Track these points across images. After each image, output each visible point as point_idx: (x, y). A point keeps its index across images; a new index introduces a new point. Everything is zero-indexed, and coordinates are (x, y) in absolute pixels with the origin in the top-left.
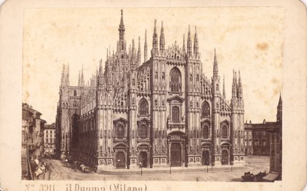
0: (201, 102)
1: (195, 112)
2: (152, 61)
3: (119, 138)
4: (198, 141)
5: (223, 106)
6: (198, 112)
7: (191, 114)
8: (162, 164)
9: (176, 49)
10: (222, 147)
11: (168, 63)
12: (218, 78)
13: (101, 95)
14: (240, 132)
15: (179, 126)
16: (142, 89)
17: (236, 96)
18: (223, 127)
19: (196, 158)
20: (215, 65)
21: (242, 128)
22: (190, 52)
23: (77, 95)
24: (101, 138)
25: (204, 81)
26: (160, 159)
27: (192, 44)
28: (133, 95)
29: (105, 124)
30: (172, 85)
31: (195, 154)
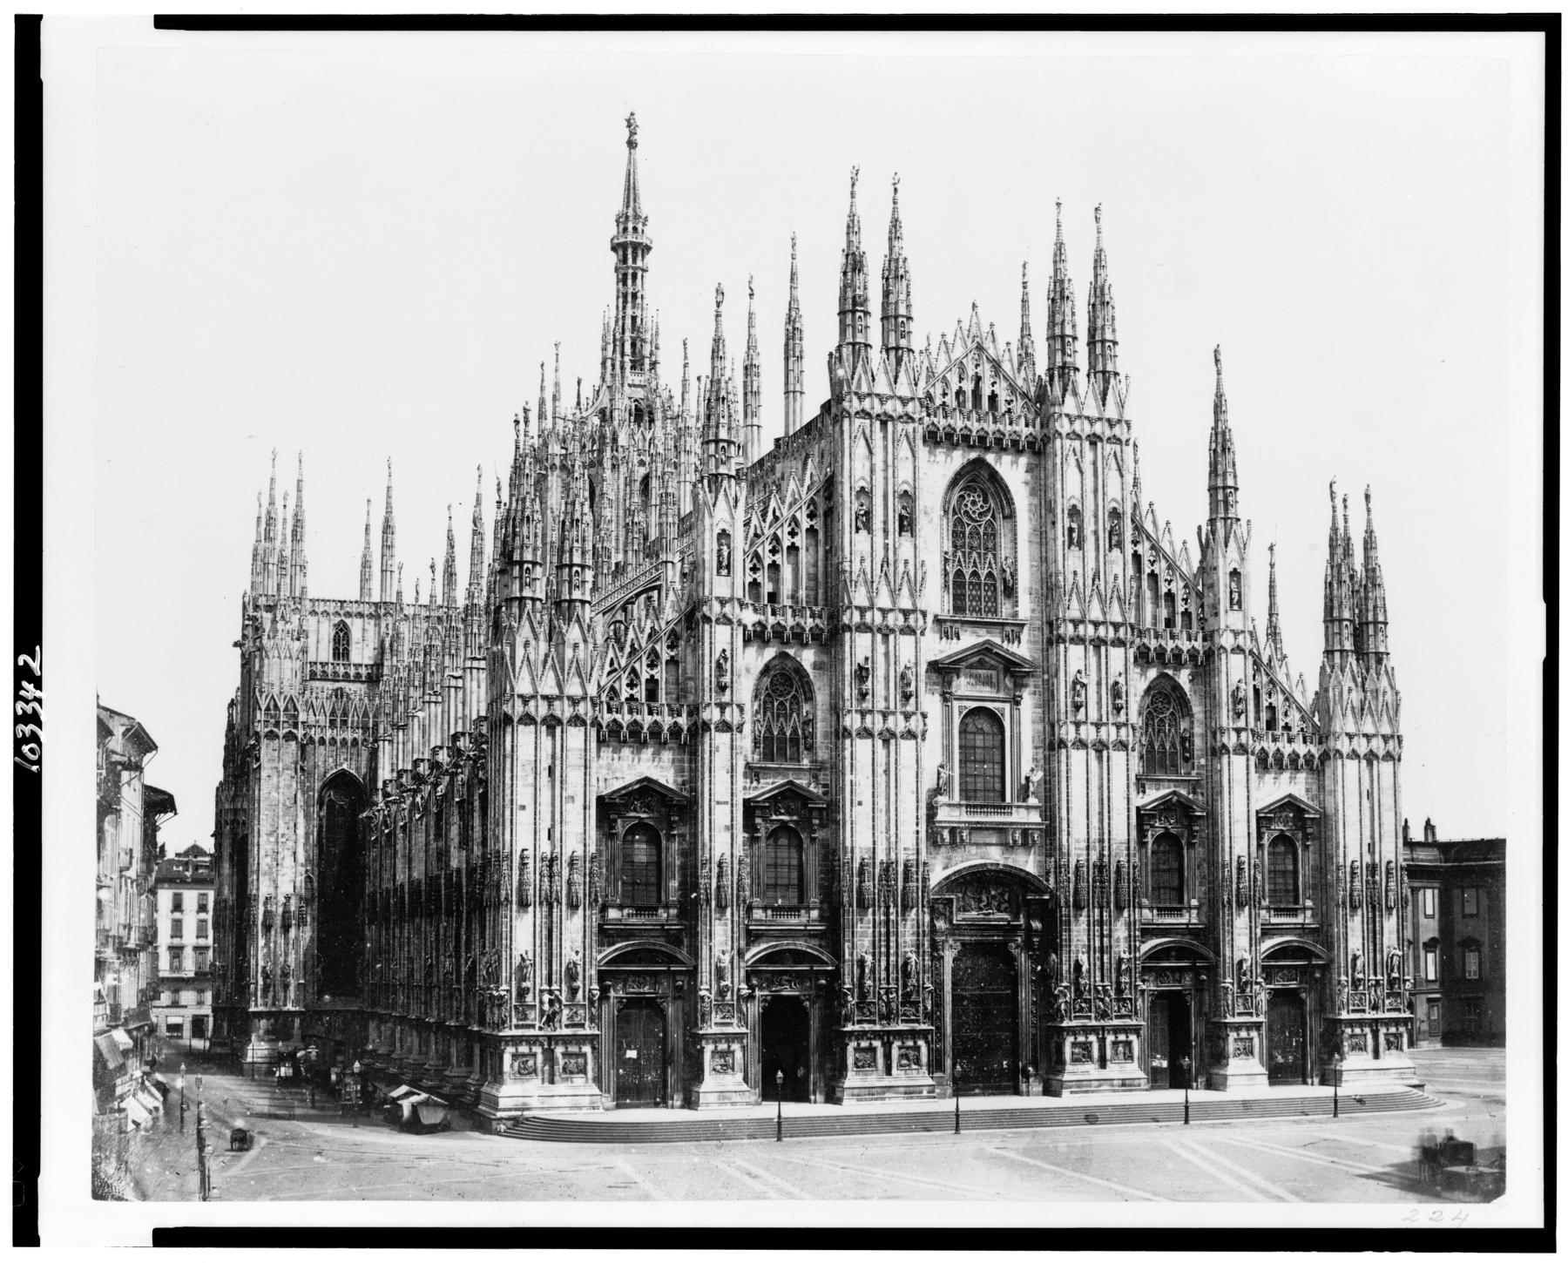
0: (1138, 683)
1: (1100, 747)
2: (838, 420)
4: (1120, 931)
5: (1271, 708)
6: (1122, 745)
7: (1078, 756)
8: (899, 1077)
9: (980, 348)
10: (1269, 973)
11: (933, 438)
12: (1239, 530)
13: (525, 632)
14: (1381, 877)
15: (1001, 829)
16: (773, 597)
18: (1274, 843)
19: (1110, 1038)
20: (1221, 445)
21: (1390, 851)
22: (1064, 367)
23: (355, 657)
24: (523, 905)
26: (887, 1046)
27: (1080, 334)
28: (720, 638)
29: (550, 809)
30: (959, 574)
31: (1104, 1015)
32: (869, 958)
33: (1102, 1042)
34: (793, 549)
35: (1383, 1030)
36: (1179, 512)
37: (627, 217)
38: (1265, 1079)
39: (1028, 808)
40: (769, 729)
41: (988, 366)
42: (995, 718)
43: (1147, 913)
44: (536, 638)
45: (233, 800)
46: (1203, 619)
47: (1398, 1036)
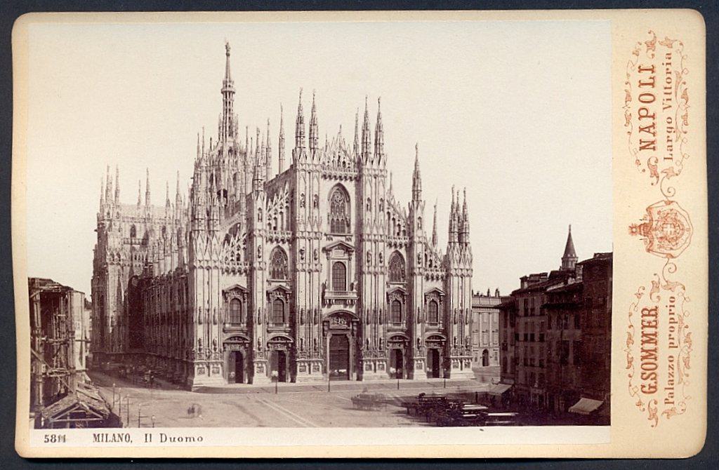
0: (389, 253)
3: (233, 324)
4: (381, 331)
5: (431, 261)
6: (382, 273)
7: (368, 277)
9: (340, 147)
10: (427, 342)
11: (324, 177)
13: (199, 241)
14: (464, 314)
16: (275, 228)
17: (456, 240)
19: (377, 363)
23: (138, 237)
26: (309, 365)
27: (371, 143)
28: (258, 241)
29: (209, 292)
32: (304, 339)
33: (375, 364)
34: (281, 213)
36: (403, 199)
37: (227, 81)
38: (426, 377)
40: (274, 269)
41: (343, 153)
43: (390, 325)
46: (409, 233)
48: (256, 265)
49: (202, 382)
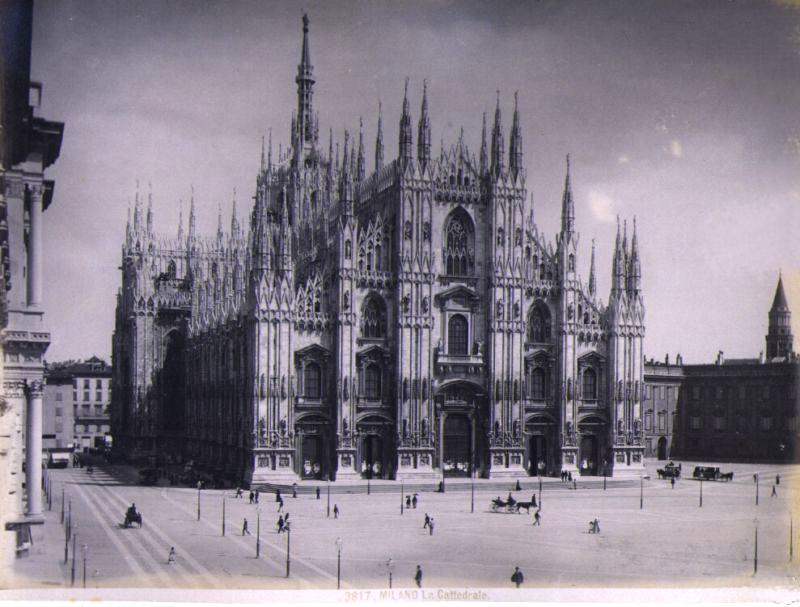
0: (527, 306)
4: (516, 409)
6: (519, 331)
7: (499, 336)
9: (461, 157)
11: (439, 198)
13: (263, 284)
16: (369, 267)
19: (511, 455)
21: (638, 375)
24: (263, 397)
25: (537, 244)
28: (346, 286)
30: (450, 257)
32: (408, 420)
35: (632, 453)
39: (478, 357)
40: (367, 323)
42: (464, 319)
43: (528, 402)
44: (268, 286)
45: (122, 341)
47: (638, 456)
48: (342, 318)
49: (265, 477)
